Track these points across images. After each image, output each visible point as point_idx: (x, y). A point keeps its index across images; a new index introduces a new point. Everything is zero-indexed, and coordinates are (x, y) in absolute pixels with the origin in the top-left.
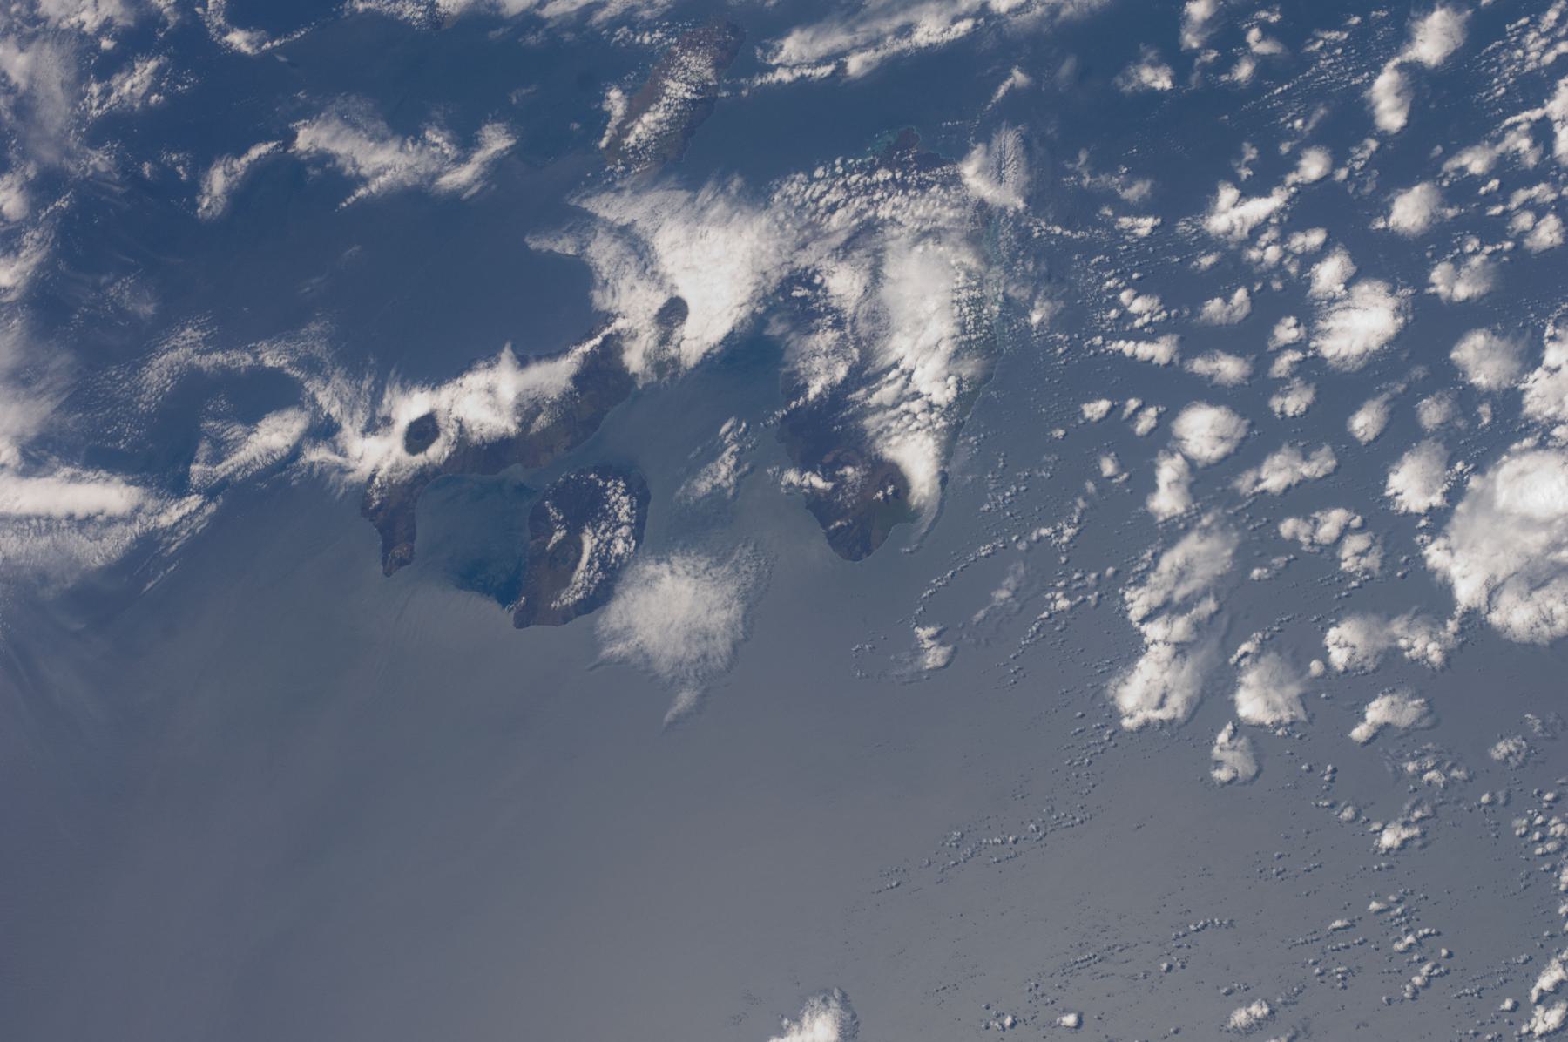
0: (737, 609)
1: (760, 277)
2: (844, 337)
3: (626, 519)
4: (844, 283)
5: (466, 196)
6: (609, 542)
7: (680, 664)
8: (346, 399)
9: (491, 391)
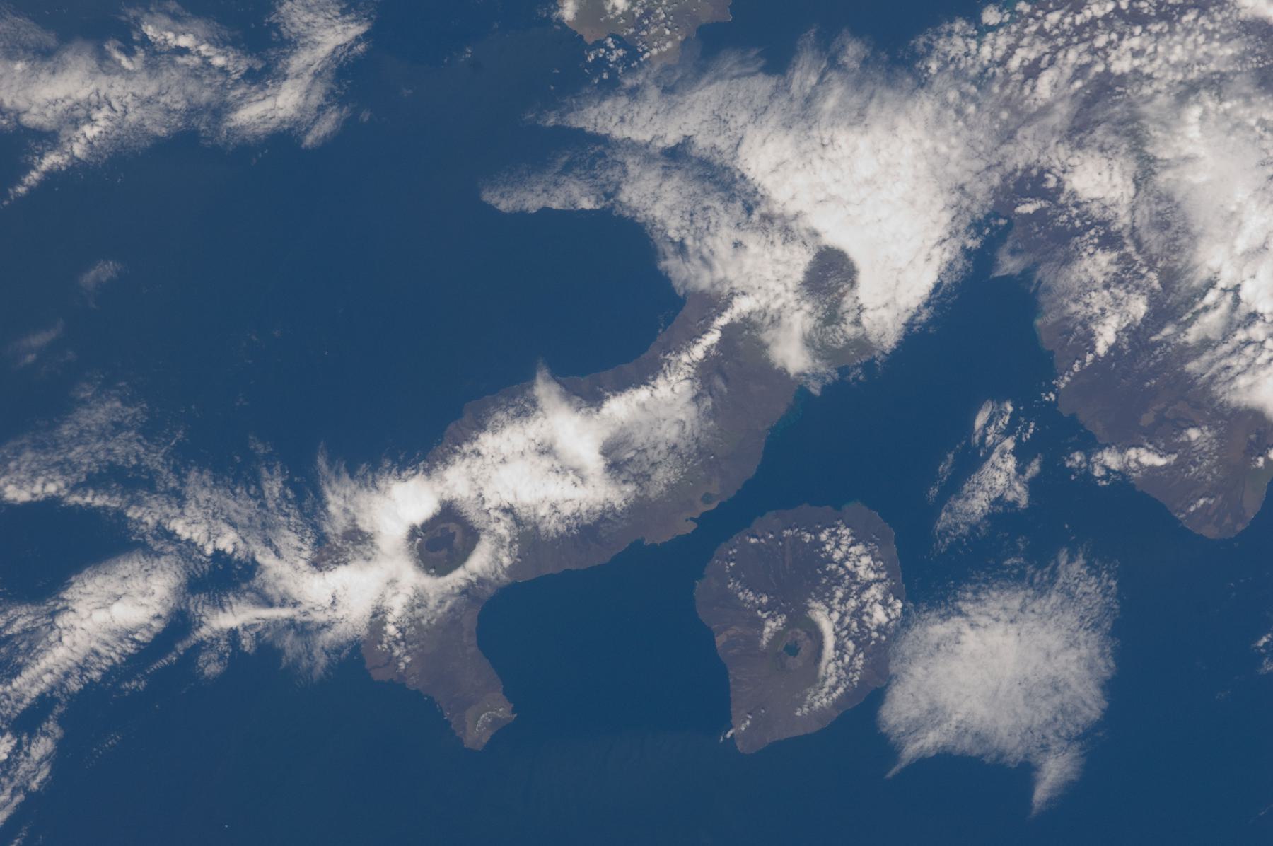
0: (1090, 645)
1: (957, 194)
2: (1121, 258)
3: (872, 576)
4: (1096, 180)
5: (309, 140)
6: (858, 613)
7: (1029, 729)
8: (237, 518)
9: (546, 450)
